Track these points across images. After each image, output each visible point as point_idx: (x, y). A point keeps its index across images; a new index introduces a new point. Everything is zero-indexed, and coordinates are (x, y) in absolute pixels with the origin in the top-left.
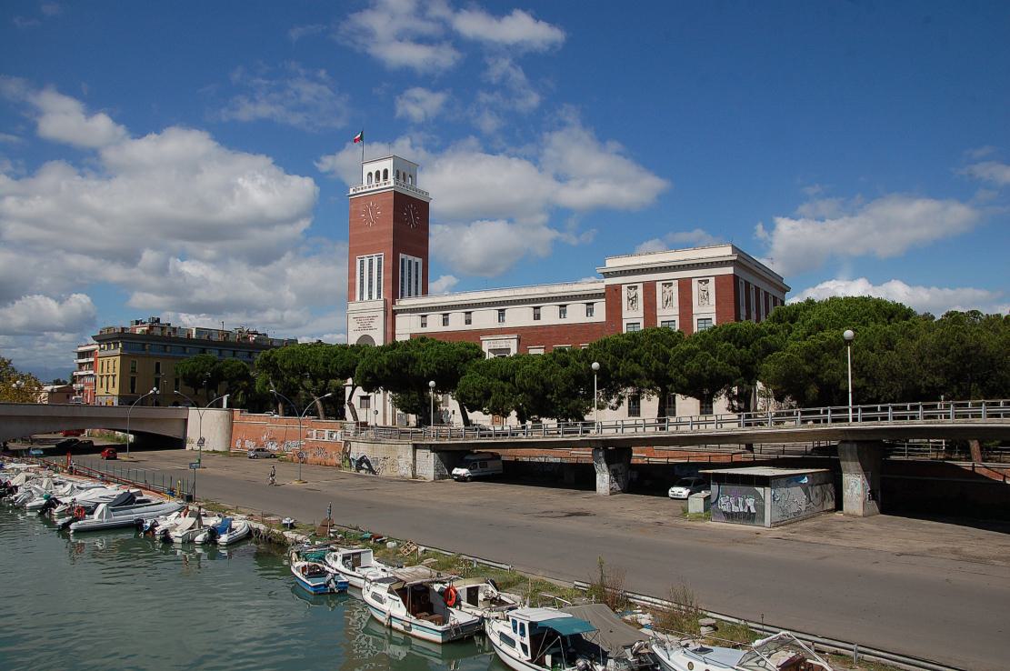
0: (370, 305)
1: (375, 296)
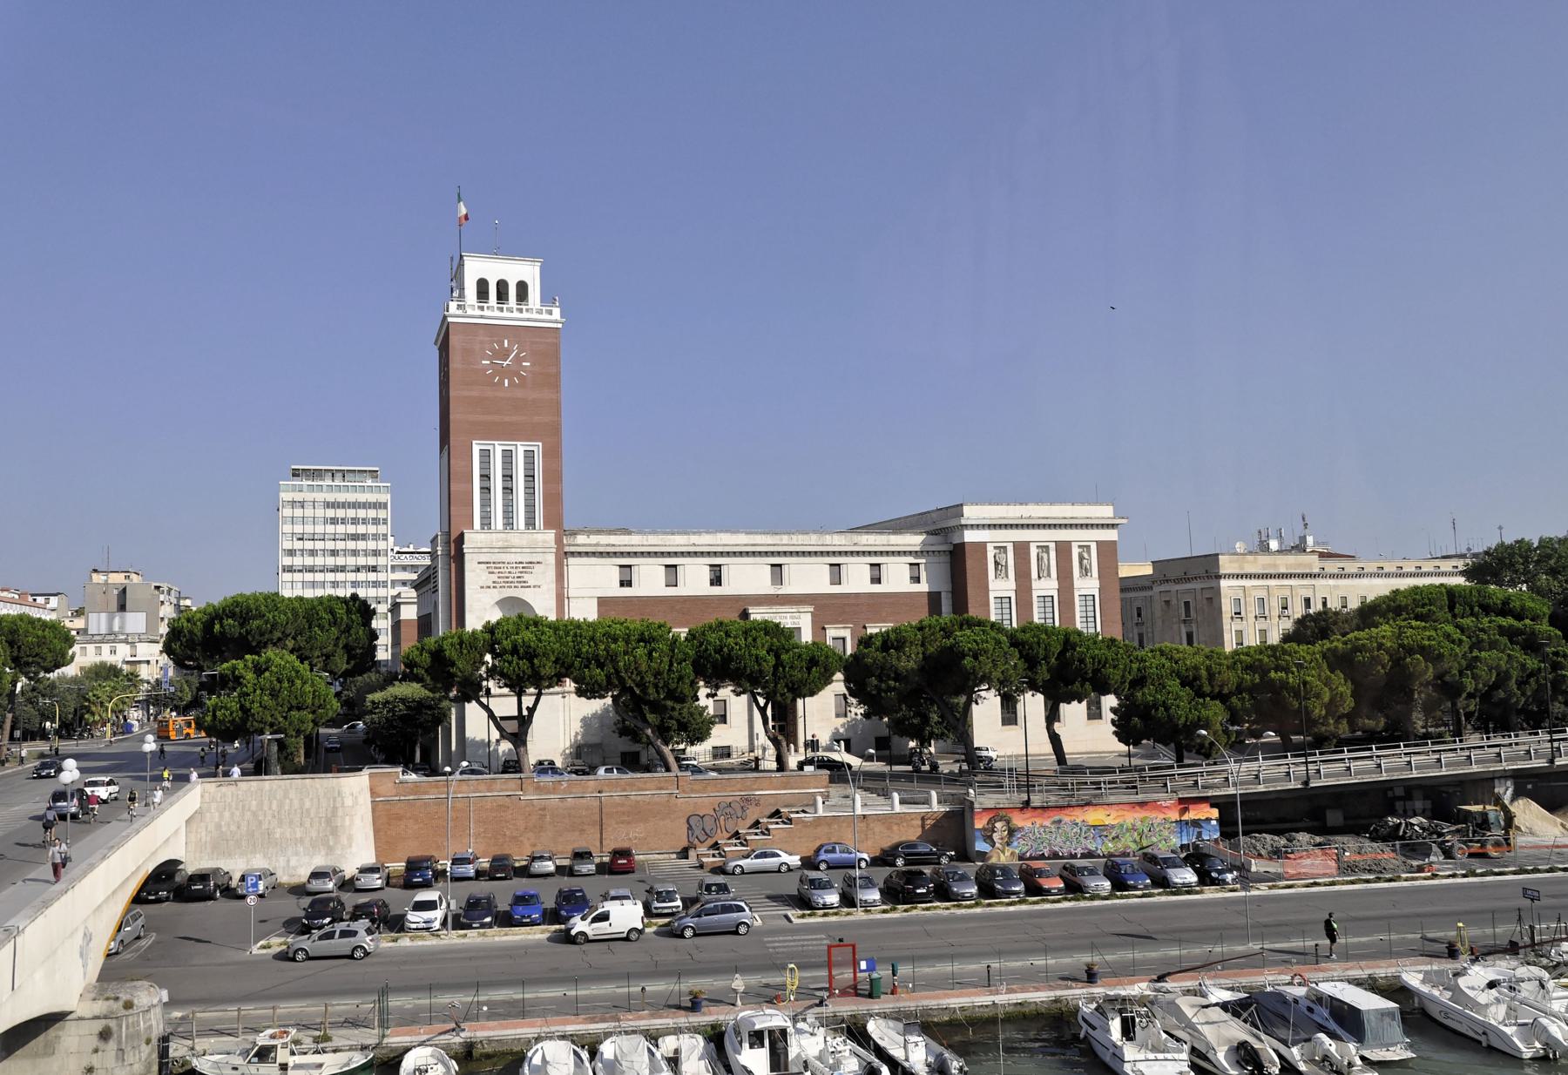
0: (514, 538)
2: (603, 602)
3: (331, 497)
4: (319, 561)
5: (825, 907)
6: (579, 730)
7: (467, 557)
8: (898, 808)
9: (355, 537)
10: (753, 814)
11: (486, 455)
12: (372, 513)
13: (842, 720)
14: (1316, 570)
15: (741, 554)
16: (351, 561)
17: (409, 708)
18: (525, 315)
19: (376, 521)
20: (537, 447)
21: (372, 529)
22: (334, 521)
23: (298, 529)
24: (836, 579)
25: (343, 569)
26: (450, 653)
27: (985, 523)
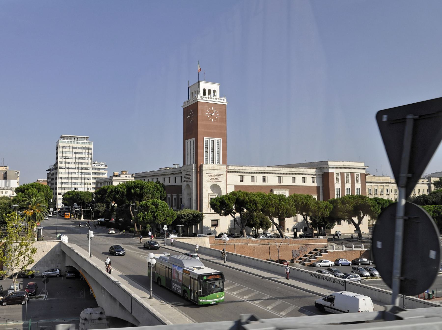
1: (216, 161)
2: (236, 186)
3: (74, 145)
4: (70, 166)
5: (367, 276)
6: (230, 224)
7: (203, 172)
8: (354, 249)
9: (82, 158)
10: (309, 250)
11: (207, 141)
12: (87, 151)
13: (295, 222)
14: (390, 181)
15: (271, 173)
16: (80, 166)
17: (194, 217)
18: (217, 100)
19: (88, 154)
20: (220, 140)
21: (87, 156)
22: (75, 153)
23: (64, 155)
24: (294, 182)
25: (78, 168)
26: (227, 201)
27: (335, 167)
